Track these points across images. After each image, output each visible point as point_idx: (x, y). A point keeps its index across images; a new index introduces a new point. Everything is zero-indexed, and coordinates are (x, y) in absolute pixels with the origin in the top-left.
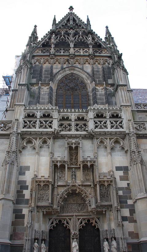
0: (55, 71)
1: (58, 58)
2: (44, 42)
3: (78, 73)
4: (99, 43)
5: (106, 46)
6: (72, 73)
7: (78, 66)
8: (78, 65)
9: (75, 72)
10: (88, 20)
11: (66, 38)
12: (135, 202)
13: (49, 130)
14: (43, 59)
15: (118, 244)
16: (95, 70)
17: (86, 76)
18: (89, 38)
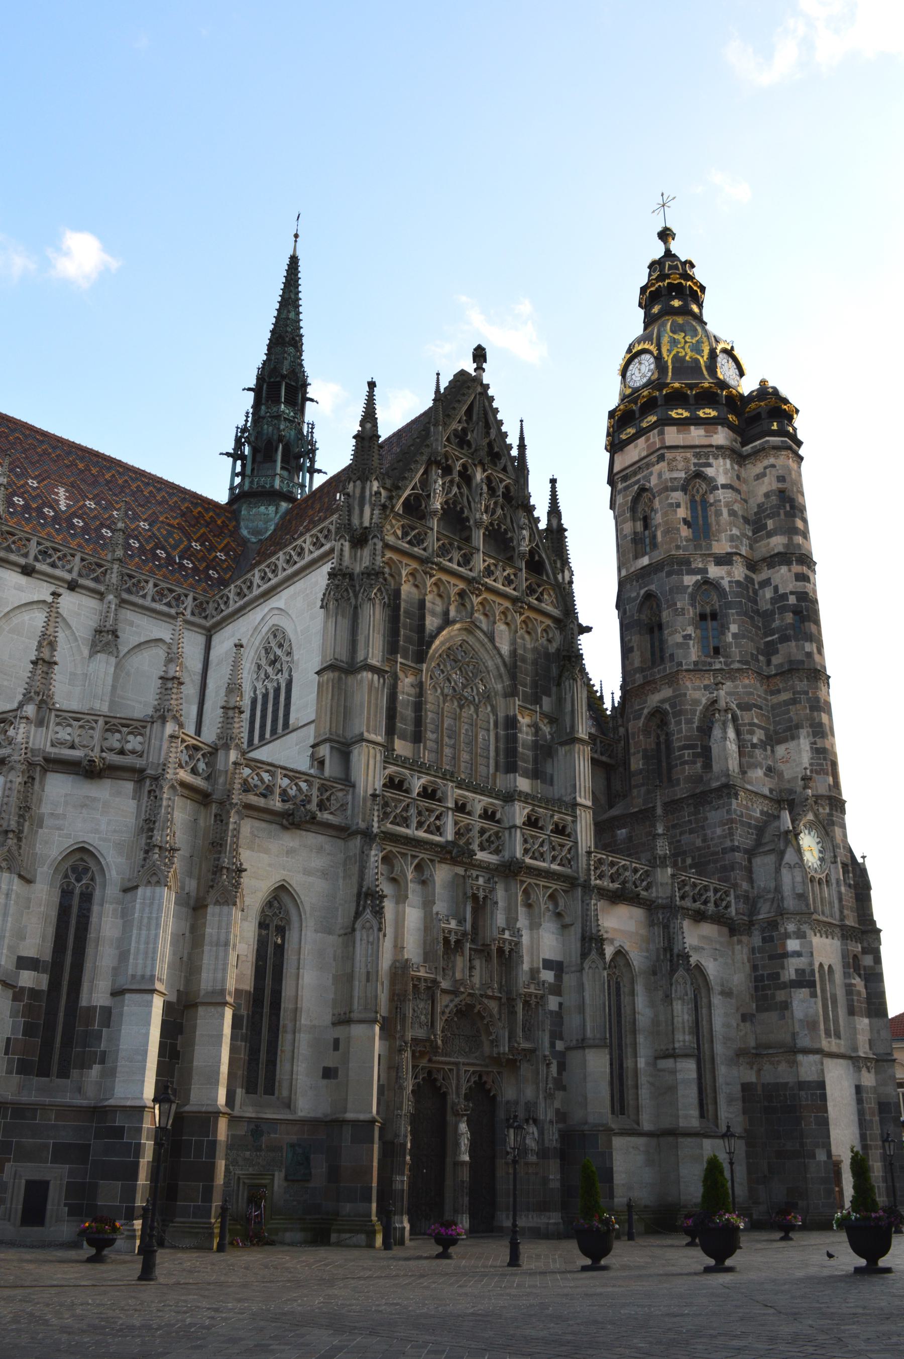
0: (431, 623)
1: (445, 577)
2: (410, 495)
3: (477, 646)
4: (540, 556)
5: (556, 579)
6: (464, 640)
7: (481, 622)
8: (482, 618)
9: (471, 640)
10: (522, 447)
11: (465, 499)
12: (568, 1049)
13: (437, 838)
14: (407, 565)
15: (541, 1133)
16: (520, 651)
17: (498, 668)
18: (524, 532)
